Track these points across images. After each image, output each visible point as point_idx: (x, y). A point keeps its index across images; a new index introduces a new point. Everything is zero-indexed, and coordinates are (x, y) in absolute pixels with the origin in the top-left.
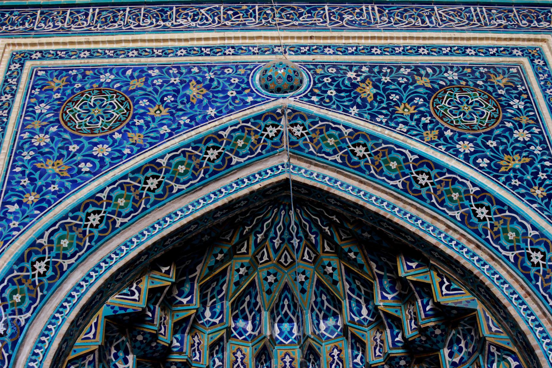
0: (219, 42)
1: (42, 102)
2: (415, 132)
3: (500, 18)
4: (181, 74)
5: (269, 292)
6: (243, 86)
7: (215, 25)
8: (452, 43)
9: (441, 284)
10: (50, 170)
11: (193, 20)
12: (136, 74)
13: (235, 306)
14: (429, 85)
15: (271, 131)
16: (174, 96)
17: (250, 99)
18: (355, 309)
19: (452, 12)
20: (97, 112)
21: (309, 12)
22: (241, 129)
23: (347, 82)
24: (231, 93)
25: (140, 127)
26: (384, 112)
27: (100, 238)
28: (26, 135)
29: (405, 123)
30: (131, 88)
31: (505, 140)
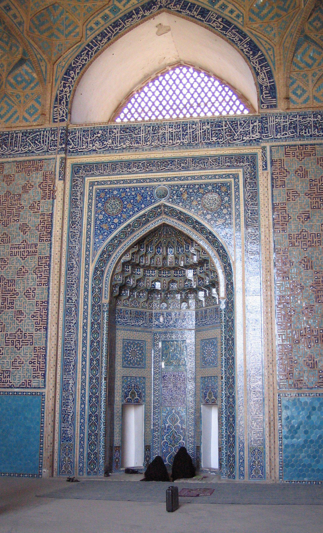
0: (145, 177)
1: (99, 202)
2: (196, 212)
3: (228, 162)
4: (135, 190)
5: (165, 243)
6: (152, 195)
7: (144, 171)
8: (212, 174)
9: (202, 252)
10: (104, 228)
11: (138, 169)
12: (123, 191)
13: (156, 247)
14: (202, 192)
15: (159, 210)
16: (133, 200)
17: (153, 201)
18: (187, 247)
19: (214, 160)
20: (114, 206)
21: (171, 163)
22: (151, 211)
23: (180, 193)
24: (148, 199)
25: (125, 212)
26: (189, 204)
27: (118, 245)
28: (97, 215)
29: (194, 208)
30: (122, 197)
31: (220, 214)
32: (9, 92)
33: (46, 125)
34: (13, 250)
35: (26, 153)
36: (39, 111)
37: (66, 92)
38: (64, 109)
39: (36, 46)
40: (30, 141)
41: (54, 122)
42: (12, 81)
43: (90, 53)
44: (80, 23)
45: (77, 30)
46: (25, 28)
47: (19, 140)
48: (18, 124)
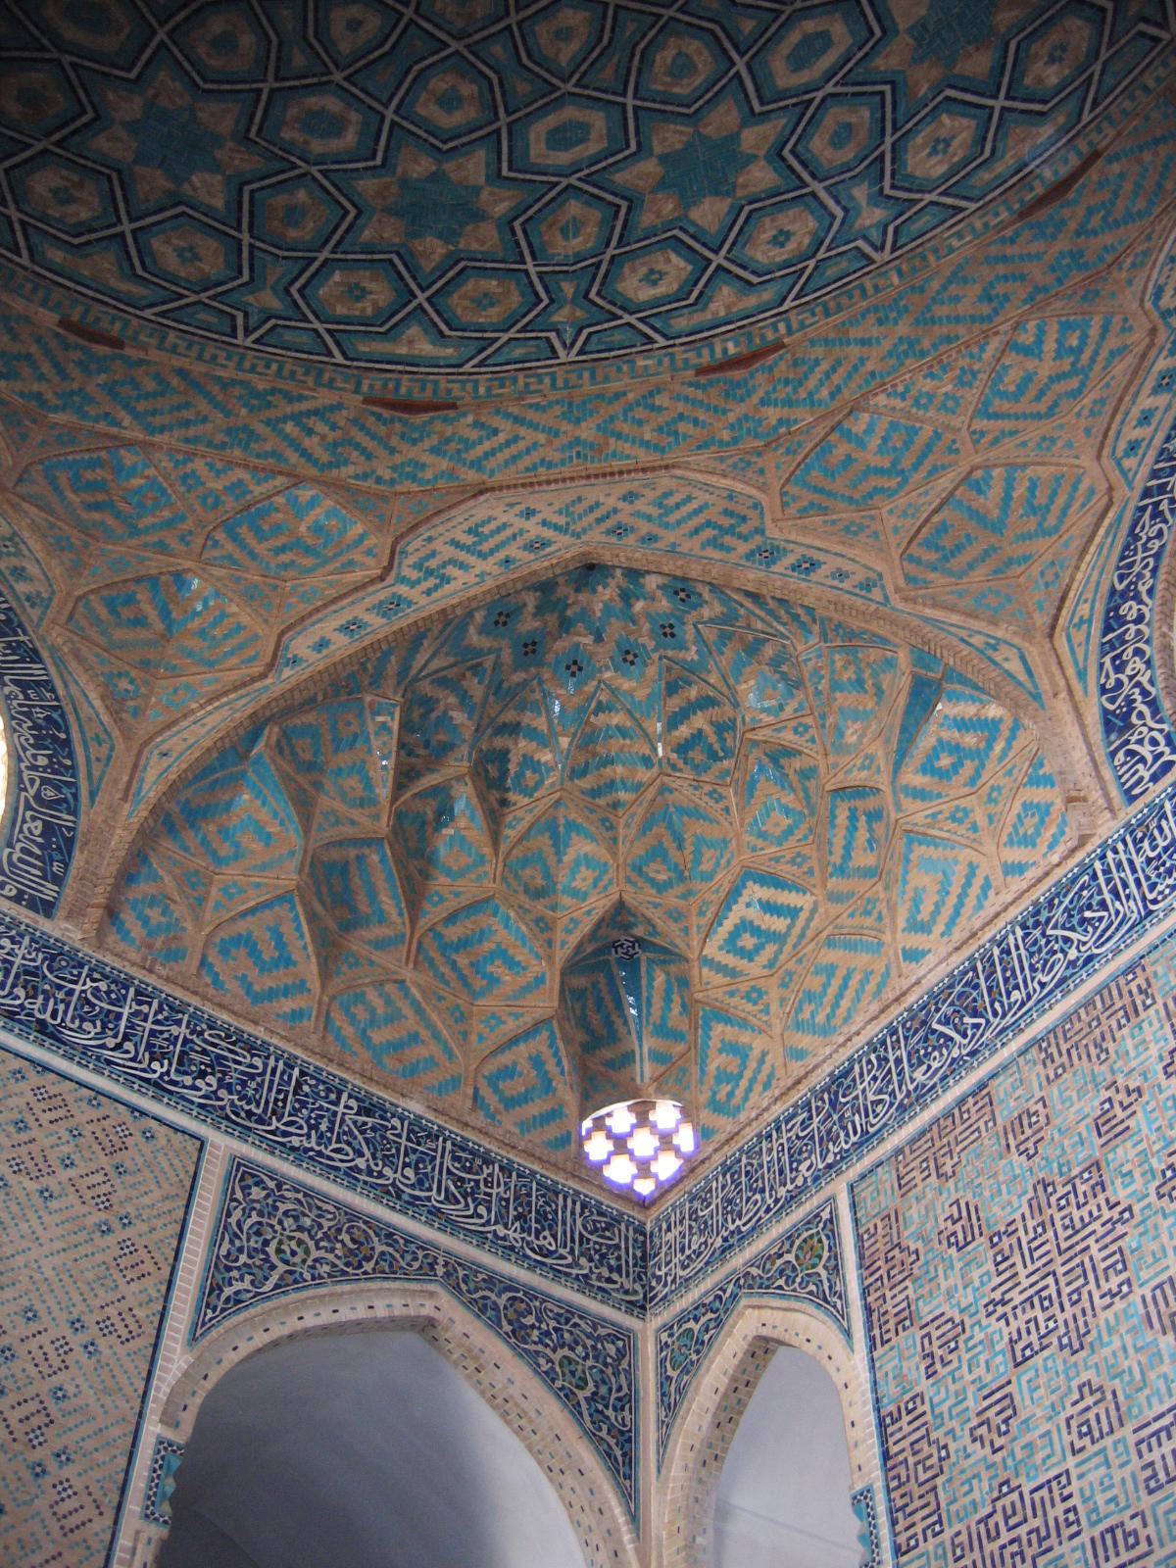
32: (919, 818)
33: (1100, 831)
34: (1155, 1456)
35: (1063, 980)
36: (1059, 803)
37: (1131, 678)
38: (1151, 729)
39: (955, 618)
40: (1063, 927)
41: (1132, 799)
42: (919, 780)
43: (1164, 506)
44: (1087, 461)
45: (1084, 486)
46: (890, 589)
47: (1019, 956)
48: (993, 904)
